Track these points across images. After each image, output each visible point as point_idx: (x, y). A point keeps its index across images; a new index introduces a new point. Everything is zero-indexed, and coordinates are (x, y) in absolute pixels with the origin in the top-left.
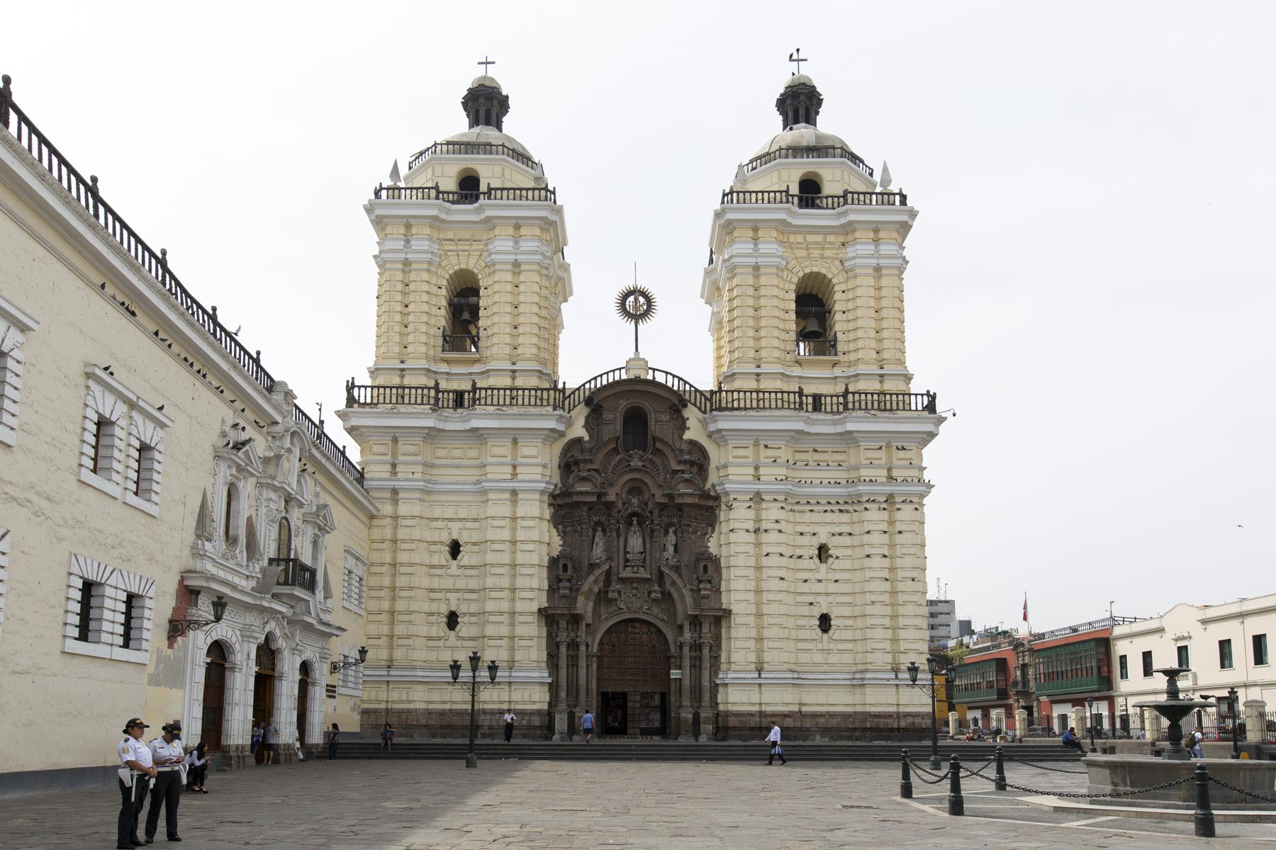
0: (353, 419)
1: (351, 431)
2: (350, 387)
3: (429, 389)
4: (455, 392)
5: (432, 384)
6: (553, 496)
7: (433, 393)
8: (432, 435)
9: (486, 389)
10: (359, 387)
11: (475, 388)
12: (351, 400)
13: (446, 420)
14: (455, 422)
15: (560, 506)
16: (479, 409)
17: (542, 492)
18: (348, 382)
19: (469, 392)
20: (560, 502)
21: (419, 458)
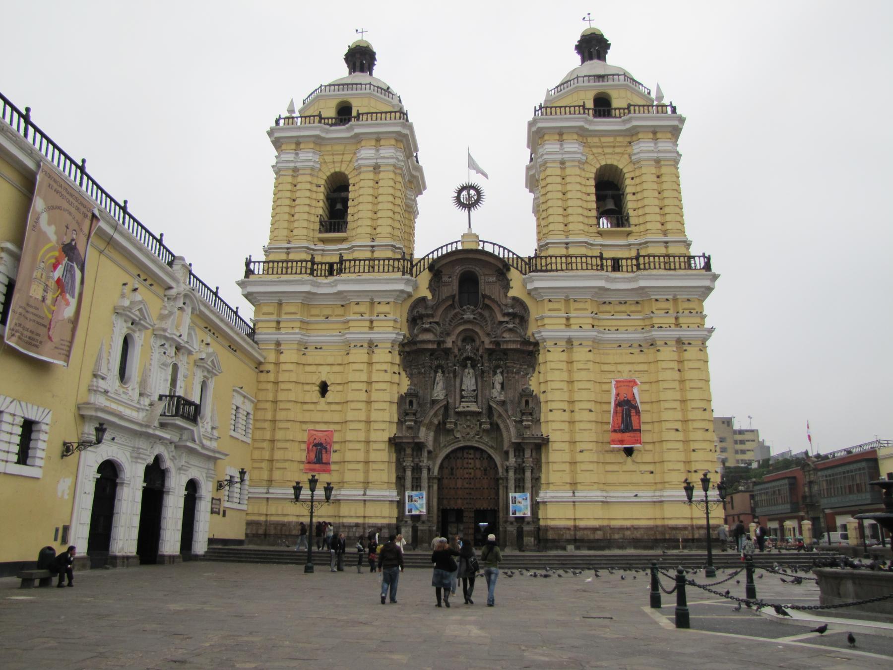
0: (248, 287)
1: (248, 296)
2: (248, 263)
3: (307, 261)
4: (325, 264)
5: (309, 258)
6: (402, 345)
7: (309, 265)
8: (308, 300)
9: (350, 261)
10: (255, 262)
11: (341, 261)
12: (249, 272)
13: (319, 285)
14: (326, 286)
15: (408, 353)
16: (344, 276)
17: (393, 342)
18: (247, 259)
19: (337, 263)
20: (407, 349)
21: (298, 317)
